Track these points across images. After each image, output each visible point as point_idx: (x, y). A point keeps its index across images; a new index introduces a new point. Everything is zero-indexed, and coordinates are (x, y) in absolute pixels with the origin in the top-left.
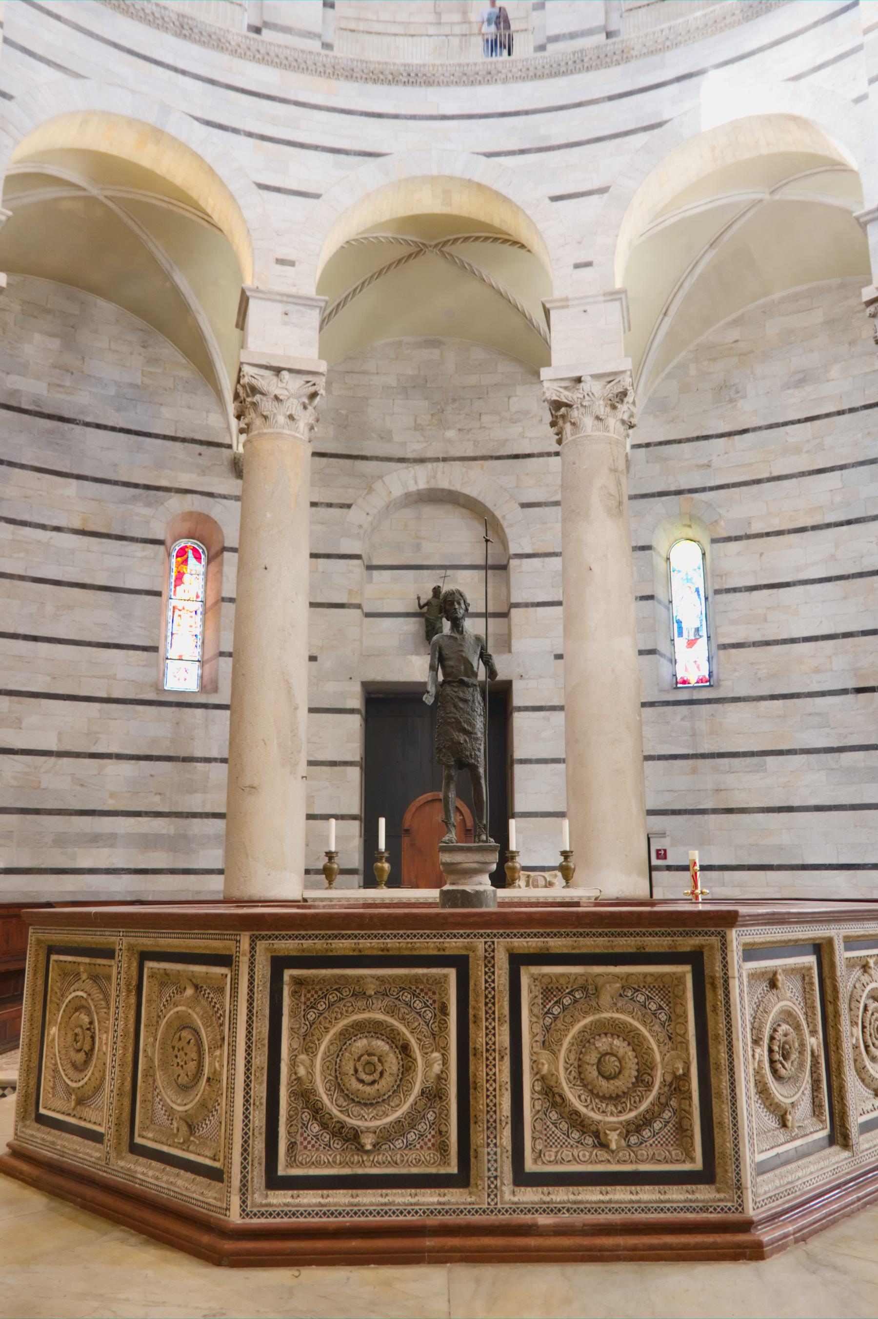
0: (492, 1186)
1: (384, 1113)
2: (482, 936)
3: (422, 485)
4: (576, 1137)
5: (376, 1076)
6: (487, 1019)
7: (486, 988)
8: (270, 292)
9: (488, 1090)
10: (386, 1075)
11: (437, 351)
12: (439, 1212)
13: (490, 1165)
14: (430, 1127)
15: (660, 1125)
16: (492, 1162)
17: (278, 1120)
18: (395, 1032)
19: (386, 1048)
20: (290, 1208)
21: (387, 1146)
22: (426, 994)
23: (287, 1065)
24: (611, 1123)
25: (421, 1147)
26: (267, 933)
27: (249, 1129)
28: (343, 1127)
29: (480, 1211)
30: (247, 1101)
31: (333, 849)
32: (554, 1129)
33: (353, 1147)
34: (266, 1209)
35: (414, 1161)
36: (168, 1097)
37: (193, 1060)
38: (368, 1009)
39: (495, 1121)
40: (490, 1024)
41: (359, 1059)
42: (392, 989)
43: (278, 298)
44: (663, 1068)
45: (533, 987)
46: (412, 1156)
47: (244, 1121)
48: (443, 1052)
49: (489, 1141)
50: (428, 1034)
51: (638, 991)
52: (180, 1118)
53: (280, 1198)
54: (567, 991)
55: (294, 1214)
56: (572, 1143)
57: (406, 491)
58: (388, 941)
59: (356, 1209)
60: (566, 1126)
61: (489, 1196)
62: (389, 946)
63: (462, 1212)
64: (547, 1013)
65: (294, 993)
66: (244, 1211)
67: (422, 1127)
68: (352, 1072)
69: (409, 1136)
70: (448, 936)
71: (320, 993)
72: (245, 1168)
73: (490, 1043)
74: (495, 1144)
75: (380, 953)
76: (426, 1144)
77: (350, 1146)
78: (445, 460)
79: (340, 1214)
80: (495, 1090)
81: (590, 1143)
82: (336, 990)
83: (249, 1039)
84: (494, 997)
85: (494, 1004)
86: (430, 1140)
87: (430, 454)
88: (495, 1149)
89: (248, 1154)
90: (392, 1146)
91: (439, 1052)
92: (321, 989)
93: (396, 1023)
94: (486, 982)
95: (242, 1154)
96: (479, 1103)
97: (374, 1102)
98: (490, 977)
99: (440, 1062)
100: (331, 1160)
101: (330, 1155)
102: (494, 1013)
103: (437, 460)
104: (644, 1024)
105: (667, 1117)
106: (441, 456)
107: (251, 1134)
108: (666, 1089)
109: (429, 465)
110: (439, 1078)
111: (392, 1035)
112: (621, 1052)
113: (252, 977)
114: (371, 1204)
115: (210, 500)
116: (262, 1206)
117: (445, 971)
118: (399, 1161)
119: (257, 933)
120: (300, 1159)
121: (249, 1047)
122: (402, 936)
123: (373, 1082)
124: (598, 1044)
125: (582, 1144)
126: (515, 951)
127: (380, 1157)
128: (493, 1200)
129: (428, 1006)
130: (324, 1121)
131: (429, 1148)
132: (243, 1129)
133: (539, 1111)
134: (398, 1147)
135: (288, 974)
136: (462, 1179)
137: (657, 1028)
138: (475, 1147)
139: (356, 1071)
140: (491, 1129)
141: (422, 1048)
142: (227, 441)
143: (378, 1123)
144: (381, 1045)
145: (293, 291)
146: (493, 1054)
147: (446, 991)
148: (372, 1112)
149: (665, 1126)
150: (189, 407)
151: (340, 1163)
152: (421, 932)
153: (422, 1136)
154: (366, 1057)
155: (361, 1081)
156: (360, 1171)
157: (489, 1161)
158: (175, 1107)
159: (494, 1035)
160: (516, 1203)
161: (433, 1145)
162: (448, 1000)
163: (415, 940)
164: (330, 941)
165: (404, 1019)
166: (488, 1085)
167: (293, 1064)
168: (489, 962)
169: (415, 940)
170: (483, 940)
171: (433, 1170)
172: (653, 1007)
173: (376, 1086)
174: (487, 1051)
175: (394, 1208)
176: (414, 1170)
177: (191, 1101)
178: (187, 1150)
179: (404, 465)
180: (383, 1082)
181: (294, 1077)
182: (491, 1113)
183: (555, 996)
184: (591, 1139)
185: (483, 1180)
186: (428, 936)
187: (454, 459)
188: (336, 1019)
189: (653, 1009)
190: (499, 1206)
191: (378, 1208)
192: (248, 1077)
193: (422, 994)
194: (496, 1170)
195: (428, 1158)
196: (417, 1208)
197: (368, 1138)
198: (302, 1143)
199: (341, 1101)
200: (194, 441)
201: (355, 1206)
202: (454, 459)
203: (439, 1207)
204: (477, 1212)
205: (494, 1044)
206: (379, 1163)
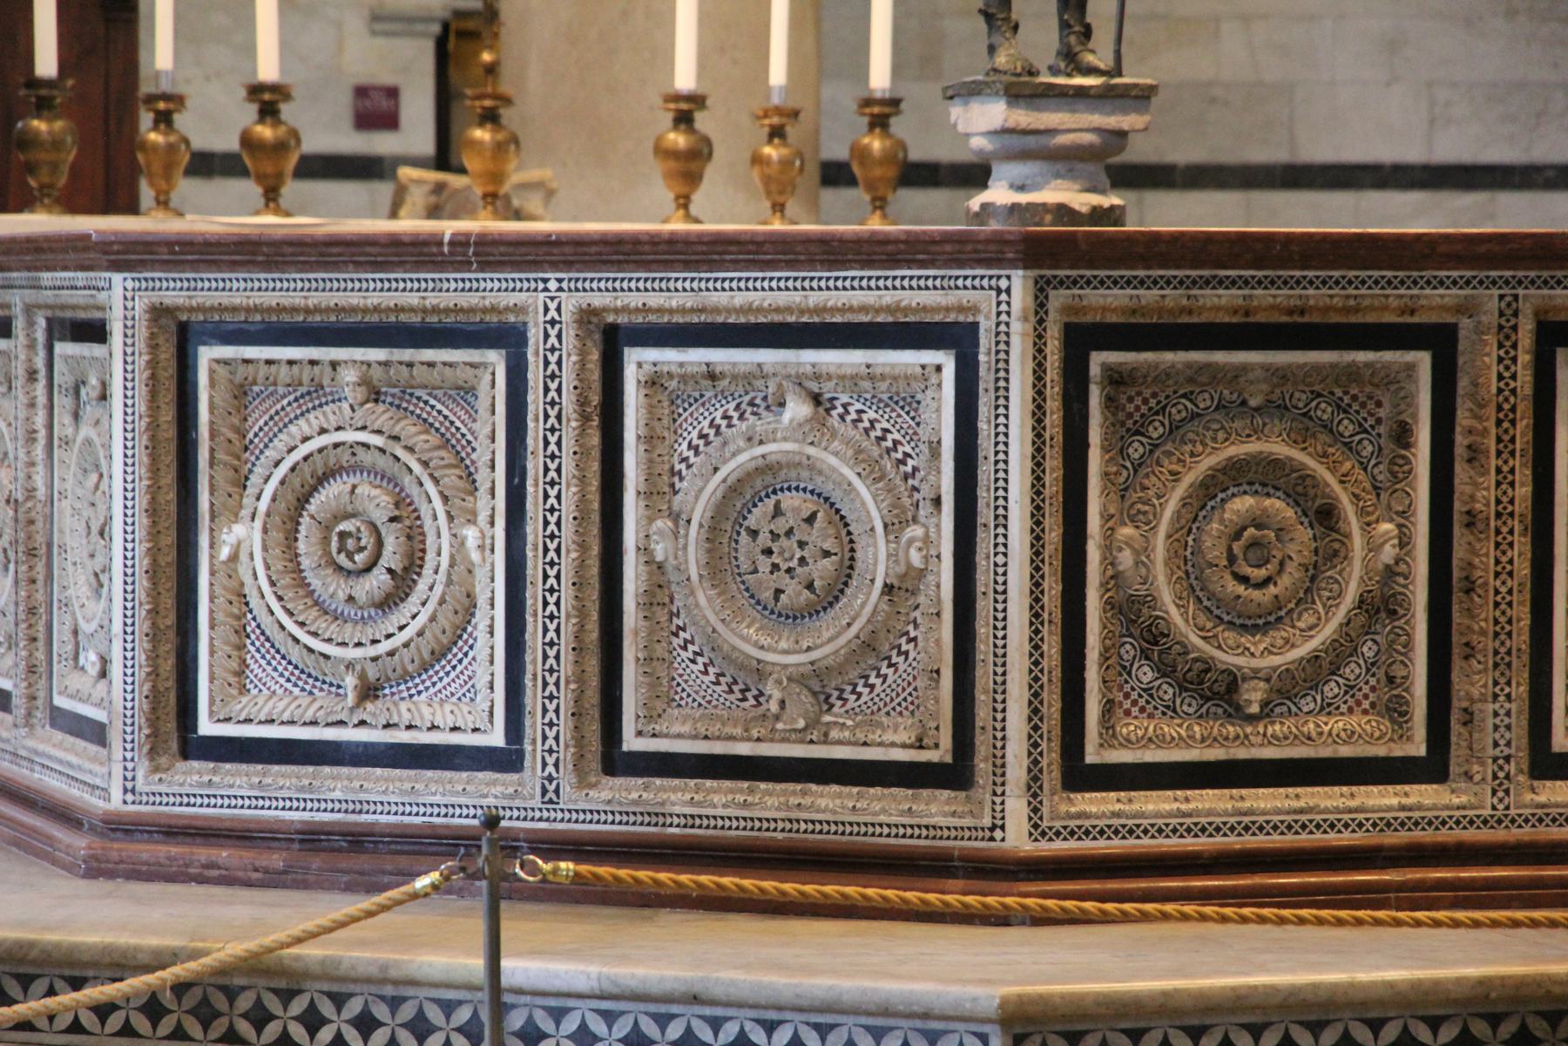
0: (1501, 775)
1: (1287, 641)
2: (1494, 283)
5: (1271, 568)
6: (1499, 453)
7: (1500, 391)
9: (1497, 592)
10: (1290, 567)
12: (1403, 824)
13: (1497, 736)
14: (1368, 670)
16: (1502, 729)
17: (1083, 656)
18: (1309, 482)
19: (1290, 513)
20: (1123, 821)
21: (1285, 708)
22: (1363, 405)
23: (1100, 547)
25: (1351, 710)
26: (1068, 272)
27: (1042, 671)
28: (1207, 671)
29: (1478, 822)
30: (1037, 615)
31: (268, 69)
33: (1220, 711)
34: (1079, 822)
35: (1343, 734)
36: (746, 639)
37: (827, 554)
38: (1257, 432)
39: (1509, 653)
40: (1506, 462)
41: (1238, 535)
42: (1297, 395)
46: (1336, 724)
47: (1031, 655)
48: (1402, 521)
49: (1497, 690)
50: (1368, 486)
52: (790, 679)
53: (1097, 804)
55: (1131, 832)
58: (1311, 292)
59: (1246, 819)
61: (1494, 792)
62: (1312, 302)
63: (1444, 823)
65: (1110, 403)
66: (1036, 826)
67: (1351, 670)
68: (1225, 563)
69: (1326, 688)
70: (1428, 283)
71: (1153, 402)
72: (1036, 745)
73: (1505, 499)
74: (1508, 696)
75: (1285, 319)
76: (1359, 703)
77: (1213, 709)
79: (1218, 829)
80: (1510, 592)
82: (1184, 396)
83: (1038, 493)
84: (1513, 409)
85: (1513, 422)
86: (1366, 697)
88: (1507, 705)
89: (1041, 719)
90: (1294, 709)
91: (1391, 520)
92: (1154, 395)
93: (1311, 463)
94: (1500, 377)
95: (1030, 719)
96: (1464, 622)
97: (1261, 622)
98: (1507, 368)
99: (1396, 541)
100: (1183, 733)
101: (1180, 726)
102: (1513, 440)
107: (1045, 679)
110: (1390, 572)
111: (1300, 489)
113: (1040, 365)
114: (1278, 812)
116: (1071, 816)
117: (1411, 356)
118: (1314, 735)
119: (1049, 273)
121: (1038, 508)
122: (1337, 283)
123: (1267, 581)
126: (1552, 317)
127: (1277, 727)
128: (1501, 800)
130: (1169, 659)
131: (1365, 712)
132: (1031, 671)
134: (1306, 709)
135: (1098, 360)
136: (1433, 768)
138: (1465, 704)
139: (1232, 559)
140: (1502, 667)
141: (1362, 512)
143: (1276, 660)
144: (1277, 506)
146: (1509, 522)
147: (1410, 400)
148: (1260, 641)
151: (1203, 740)
152: (1376, 274)
153: (1352, 687)
154: (1251, 531)
155: (1244, 580)
156: (1242, 753)
157: (1496, 728)
158: (770, 657)
159: (1512, 484)
160: (1543, 806)
161: (1373, 705)
162: (1415, 416)
163: (1363, 291)
164: (1195, 292)
165: (1325, 455)
166: (1498, 583)
167: (1109, 548)
168: (1507, 337)
169: (1363, 291)
170: (1496, 292)
171: (1380, 751)
173: (1272, 590)
174: (1498, 515)
175: (1318, 818)
176: (1345, 751)
177: (830, 640)
178: (825, 740)
180: (1285, 581)
181: (1110, 573)
182: (1503, 637)
185: (1483, 764)
186: (1389, 283)
188: (1192, 455)
190: (1513, 812)
191: (1289, 818)
192: (1037, 569)
193: (1356, 407)
194: (1508, 744)
196: (1361, 816)
197: (1255, 690)
198: (1121, 704)
199: (1202, 619)
201: (1245, 814)
203: (1402, 815)
204: (1471, 822)
205: (1512, 502)
206: (1278, 739)
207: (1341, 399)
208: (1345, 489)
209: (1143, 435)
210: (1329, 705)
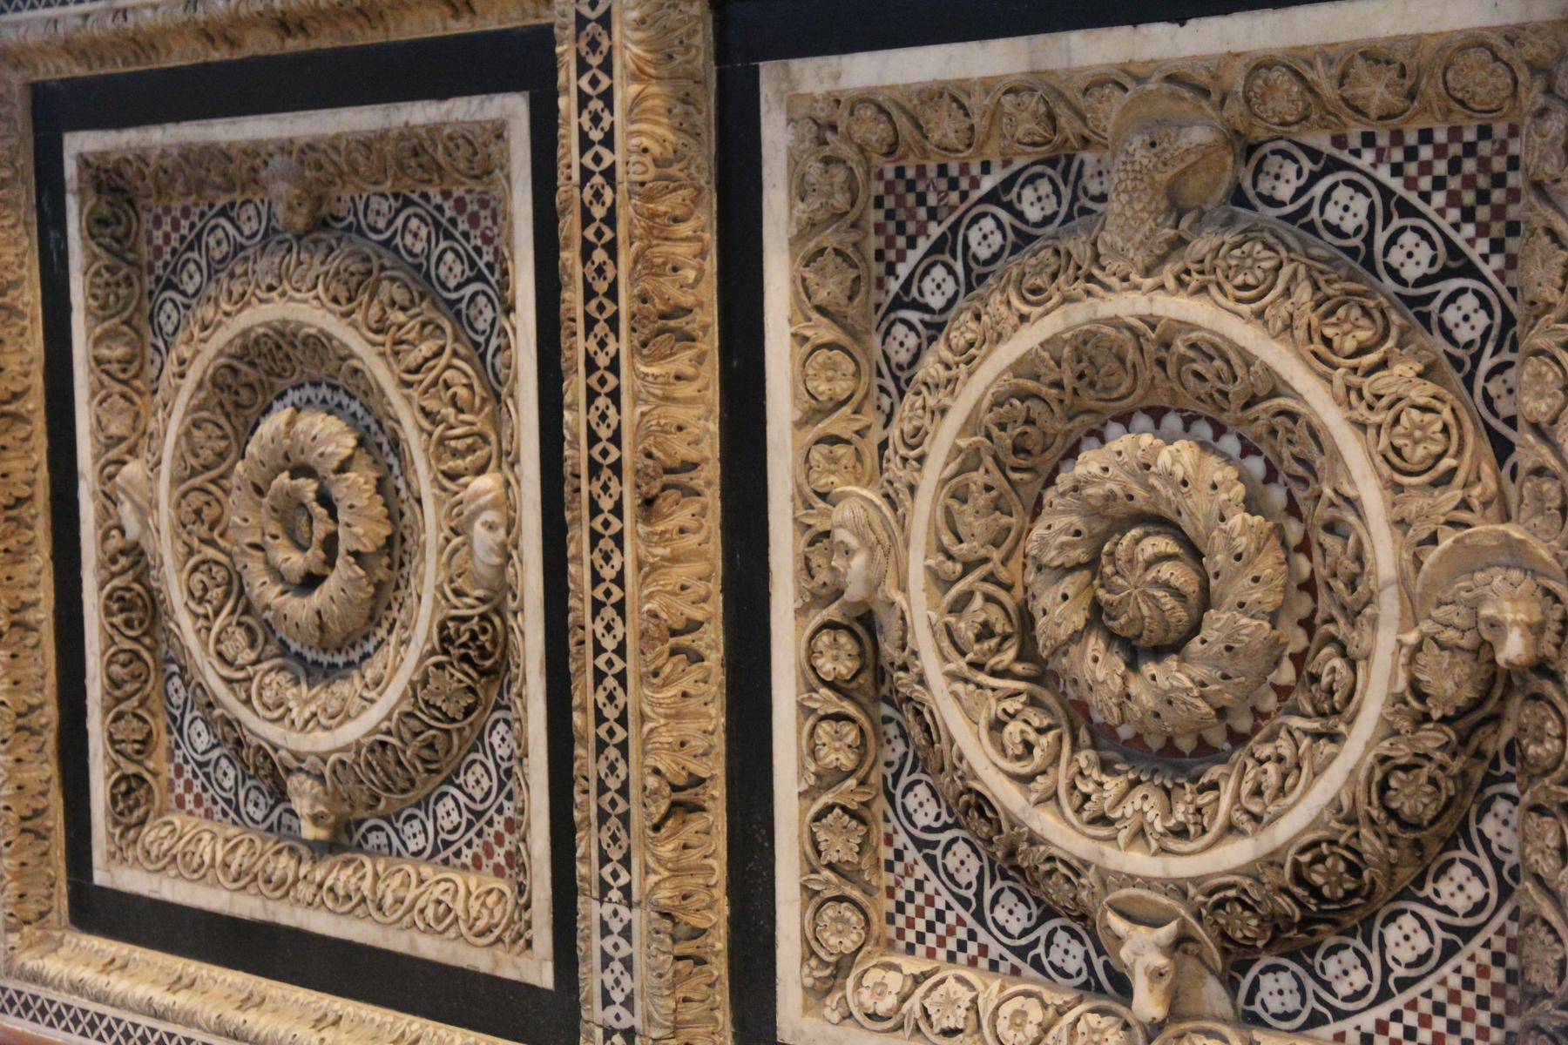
4: (1015, 927)
15: (1421, 942)
24: (1131, 879)
25: (476, 859)
32: (922, 870)
39: (624, 791)
44: (1412, 612)
45: (814, 169)
46: (436, 884)
51: (1335, 165)
54: (987, 184)
56: (995, 950)
60: (973, 864)
64: (897, 303)
80: (621, 650)
81: (1072, 966)
82: (223, 212)
84: (611, 219)
90: (396, 842)
102: (612, 293)
104: (1323, 356)
105: (1460, 903)
108: (1430, 739)
112: (1197, 509)
120: (149, 839)
124: (1090, 462)
125: (1037, 964)
129: (480, 277)
133: (841, 775)
137: (1402, 376)
149: (1449, 950)
153: (479, 815)
171: (478, 959)
172: (1412, 258)
174: (594, 469)
176: (429, 948)
181: (115, 542)
183: (933, 214)
184: (1076, 948)
189: (1411, 272)
194: (628, 1003)
195: (475, 906)
207: (440, 208)
208: (408, 398)
209: (176, 288)
210: (447, 844)
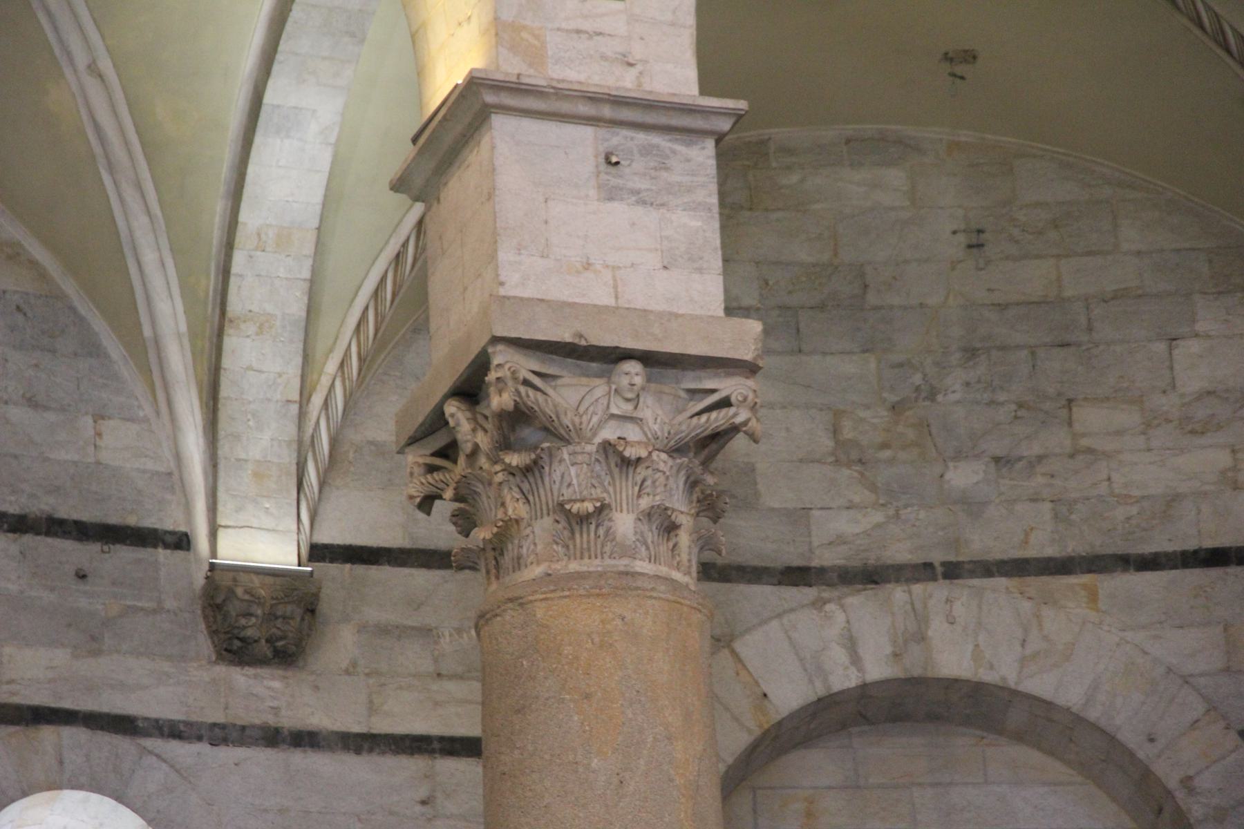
3: (877, 669)
8: (559, 93)
11: (896, 177)
43: (584, 109)
57: (821, 691)
78: (952, 571)
87: (900, 553)
103: (925, 571)
106: (937, 557)
109: (898, 593)
115: (123, 744)
142: (170, 522)
145: (625, 82)
150: (32, 403)
179: (808, 594)
187: (988, 569)
200: (54, 526)
202: (988, 569)
